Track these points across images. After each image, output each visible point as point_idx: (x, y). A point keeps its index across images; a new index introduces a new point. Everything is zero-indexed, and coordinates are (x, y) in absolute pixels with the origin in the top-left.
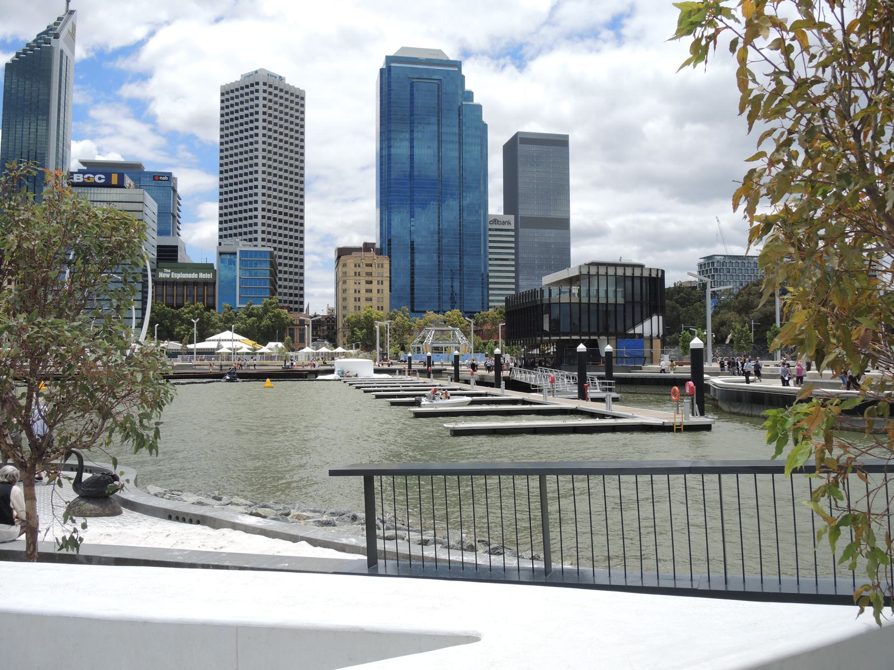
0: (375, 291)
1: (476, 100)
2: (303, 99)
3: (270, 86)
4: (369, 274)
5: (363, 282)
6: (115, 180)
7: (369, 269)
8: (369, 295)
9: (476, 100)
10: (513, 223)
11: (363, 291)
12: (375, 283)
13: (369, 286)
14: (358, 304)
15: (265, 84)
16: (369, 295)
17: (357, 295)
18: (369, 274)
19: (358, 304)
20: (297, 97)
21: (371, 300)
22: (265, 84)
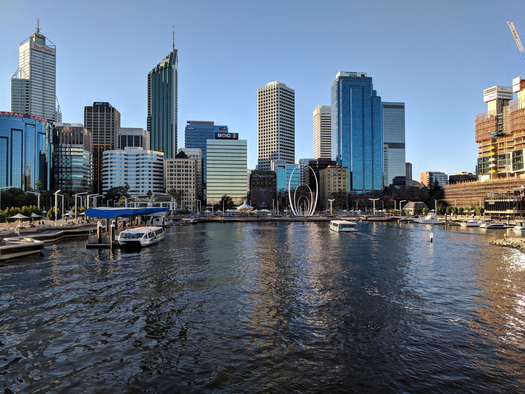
0: (342, 182)
1: (378, 95)
2: (294, 94)
3: (282, 89)
4: (340, 175)
5: (337, 178)
6: (234, 137)
7: (339, 173)
8: (340, 184)
9: (378, 95)
10: (388, 147)
11: (337, 182)
12: (342, 178)
13: (339, 180)
14: (335, 188)
15: (280, 89)
16: (340, 184)
17: (335, 184)
18: (340, 175)
19: (335, 188)
20: (292, 93)
21: (340, 186)
22: (280, 89)
